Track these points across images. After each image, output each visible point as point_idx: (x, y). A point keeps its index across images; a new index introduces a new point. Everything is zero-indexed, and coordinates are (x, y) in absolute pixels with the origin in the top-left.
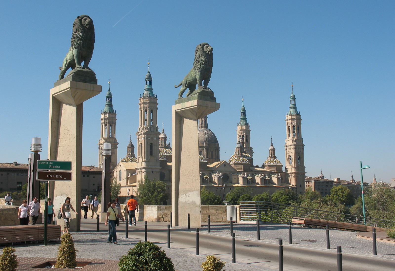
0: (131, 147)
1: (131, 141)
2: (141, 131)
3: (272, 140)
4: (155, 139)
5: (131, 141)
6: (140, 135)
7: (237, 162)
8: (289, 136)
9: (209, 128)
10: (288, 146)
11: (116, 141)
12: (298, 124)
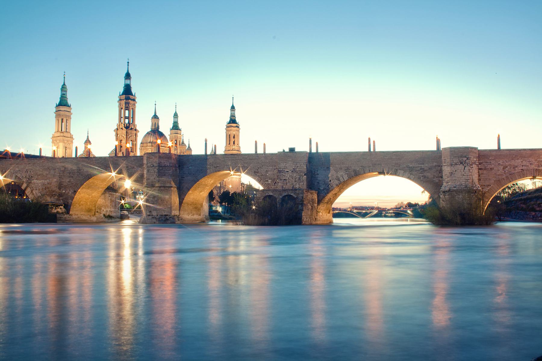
1: (88, 137)
5: (88, 137)
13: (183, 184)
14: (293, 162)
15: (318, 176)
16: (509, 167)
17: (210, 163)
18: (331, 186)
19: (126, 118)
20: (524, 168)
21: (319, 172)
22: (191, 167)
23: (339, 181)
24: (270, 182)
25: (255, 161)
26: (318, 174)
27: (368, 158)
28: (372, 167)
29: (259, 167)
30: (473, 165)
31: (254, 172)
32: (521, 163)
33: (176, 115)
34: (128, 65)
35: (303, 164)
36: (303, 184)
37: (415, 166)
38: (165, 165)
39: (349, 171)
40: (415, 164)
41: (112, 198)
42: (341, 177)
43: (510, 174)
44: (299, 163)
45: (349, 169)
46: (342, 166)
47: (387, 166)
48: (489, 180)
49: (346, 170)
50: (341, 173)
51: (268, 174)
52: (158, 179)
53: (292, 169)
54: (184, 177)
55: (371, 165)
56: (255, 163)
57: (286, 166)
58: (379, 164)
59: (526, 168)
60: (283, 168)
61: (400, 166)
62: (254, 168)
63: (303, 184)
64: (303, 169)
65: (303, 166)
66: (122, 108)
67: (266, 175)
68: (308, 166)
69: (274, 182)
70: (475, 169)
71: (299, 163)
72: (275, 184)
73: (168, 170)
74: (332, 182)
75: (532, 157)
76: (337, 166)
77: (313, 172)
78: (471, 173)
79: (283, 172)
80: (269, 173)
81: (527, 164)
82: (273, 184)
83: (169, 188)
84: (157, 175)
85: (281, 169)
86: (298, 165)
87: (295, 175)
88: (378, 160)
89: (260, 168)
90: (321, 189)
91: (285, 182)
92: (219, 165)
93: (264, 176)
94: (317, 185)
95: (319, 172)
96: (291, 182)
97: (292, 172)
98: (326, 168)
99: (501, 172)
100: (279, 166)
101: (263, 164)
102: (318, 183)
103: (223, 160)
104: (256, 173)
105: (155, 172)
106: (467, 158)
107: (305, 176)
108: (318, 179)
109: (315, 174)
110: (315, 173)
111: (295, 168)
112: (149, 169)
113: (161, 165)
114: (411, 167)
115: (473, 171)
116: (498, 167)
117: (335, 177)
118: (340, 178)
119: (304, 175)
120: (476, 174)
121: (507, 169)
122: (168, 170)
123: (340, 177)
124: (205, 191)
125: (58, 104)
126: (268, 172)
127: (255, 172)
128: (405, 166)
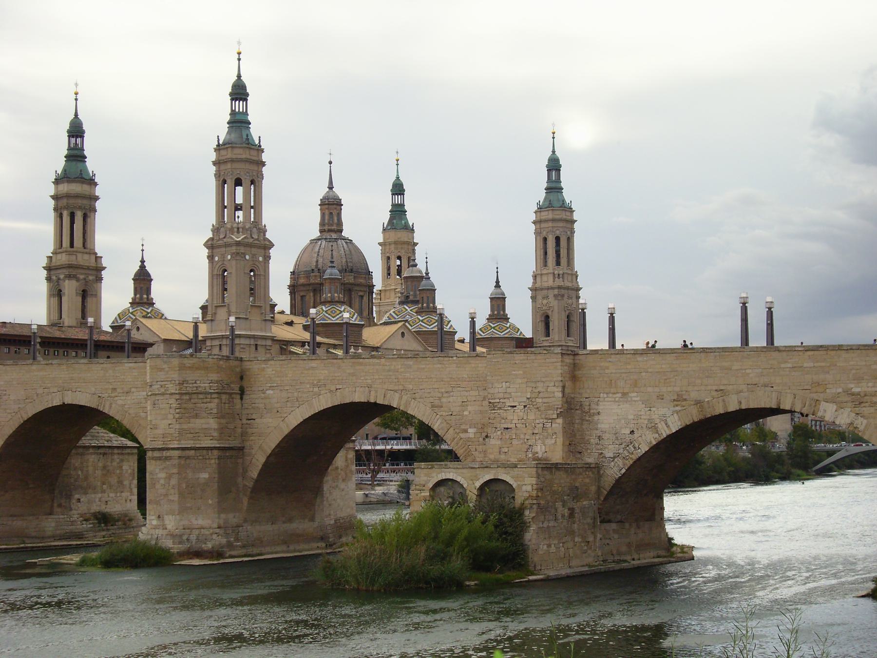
0: (143, 279)
1: (143, 261)
2: (222, 236)
3: (497, 272)
4: (261, 259)
5: (143, 261)
6: (219, 247)
7: (426, 327)
8: (545, 264)
10: (542, 289)
11: (99, 260)
12: (569, 233)
13: (252, 438)
14: (526, 380)
15: (600, 417)
17: (319, 381)
18: (635, 448)
19: (238, 208)
21: (601, 408)
22: (270, 392)
23: (657, 432)
24: (472, 436)
25: (432, 376)
26: (599, 413)
27: (734, 368)
28: (746, 394)
29: (443, 390)
31: (430, 405)
33: (398, 189)
34: (239, 59)
35: (552, 384)
36: (556, 442)
37: (870, 389)
38: (197, 387)
39: (684, 403)
40: (870, 384)
41: (109, 463)
42: (663, 423)
44: (543, 382)
45: (684, 397)
46: (664, 389)
47: (789, 391)
49: (674, 400)
50: (662, 411)
51: (466, 413)
52: (177, 426)
53: (525, 399)
54: (254, 419)
55: (744, 387)
56: (434, 380)
57: (509, 390)
58: (766, 386)
60: (501, 395)
61: (824, 392)
62: (429, 393)
63: (553, 442)
64: (554, 399)
65: (554, 393)
66: (225, 182)
67: (463, 415)
68: (567, 391)
69: (484, 435)
71: (543, 382)
72: (484, 439)
73: (205, 400)
74: (636, 435)
76: (650, 389)
77: (587, 408)
79: (500, 408)
80: (470, 408)
82: (481, 439)
83: (210, 452)
84: (177, 416)
85: (495, 399)
86: (540, 389)
87: (531, 416)
88: (762, 372)
89: (445, 395)
90: (608, 455)
91: (507, 437)
92: (340, 387)
93: (458, 417)
94: (597, 444)
95: (601, 408)
96: (522, 436)
97: (525, 406)
98: (620, 395)
100: (491, 391)
101: (455, 383)
102: (599, 438)
103: (352, 371)
104: (436, 409)
105: (170, 408)
107: (560, 421)
108: (599, 426)
109: (592, 411)
110: (590, 409)
111: (533, 396)
112: (157, 398)
113: (186, 387)
114: (858, 394)
117: (646, 422)
118: (660, 426)
119: (555, 416)
122: (205, 400)
123: (657, 421)
124: (322, 453)
125: (59, 172)
126: (467, 406)
127: (433, 406)
128: (840, 390)
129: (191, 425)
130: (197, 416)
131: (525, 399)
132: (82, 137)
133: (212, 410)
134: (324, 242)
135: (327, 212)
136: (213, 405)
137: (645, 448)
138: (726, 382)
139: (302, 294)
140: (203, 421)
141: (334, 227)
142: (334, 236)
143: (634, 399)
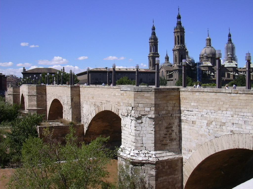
1: (167, 54)
9: (212, 46)
16: (214, 123)
20: (234, 128)
30: (144, 119)
32: (231, 118)
34: (179, 10)
43: (216, 137)
48: (191, 141)
59: (237, 129)
70: (146, 125)
75: (248, 107)
78: (139, 132)
81: (240, 122)
99: (205, 131)
106: (132, 107)
115: (144, 129)
116: (200, 120)
120: (151, 133)
121: (211, 126)
129: (31, 103)
130: (32, 101)
131: (67, 102)
132: (155, 30)
133: (35, 99)
134: (206, 48)
135: (207, 41)
136: (35, 98)
137: (90, 121)
138: (102, 99)
139: (202, 59)
140: (33, 102)
141: (209, 45)
142: (209, 46)
143: (88, 103)
